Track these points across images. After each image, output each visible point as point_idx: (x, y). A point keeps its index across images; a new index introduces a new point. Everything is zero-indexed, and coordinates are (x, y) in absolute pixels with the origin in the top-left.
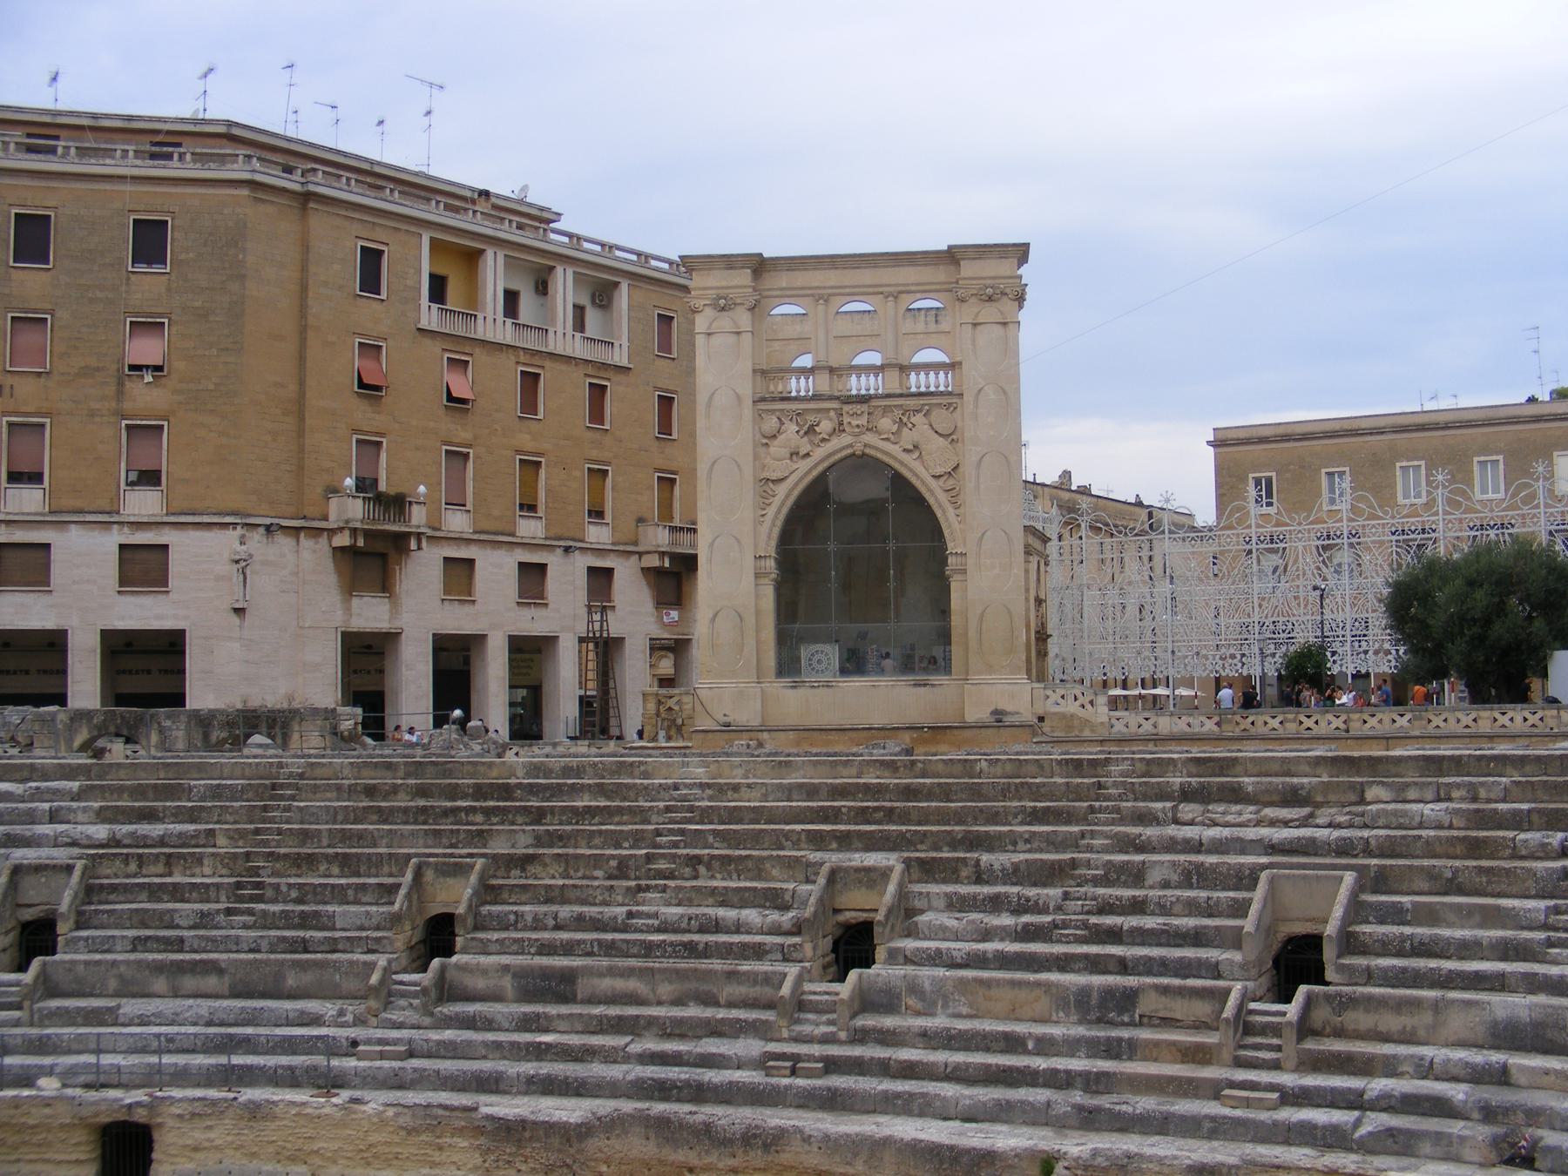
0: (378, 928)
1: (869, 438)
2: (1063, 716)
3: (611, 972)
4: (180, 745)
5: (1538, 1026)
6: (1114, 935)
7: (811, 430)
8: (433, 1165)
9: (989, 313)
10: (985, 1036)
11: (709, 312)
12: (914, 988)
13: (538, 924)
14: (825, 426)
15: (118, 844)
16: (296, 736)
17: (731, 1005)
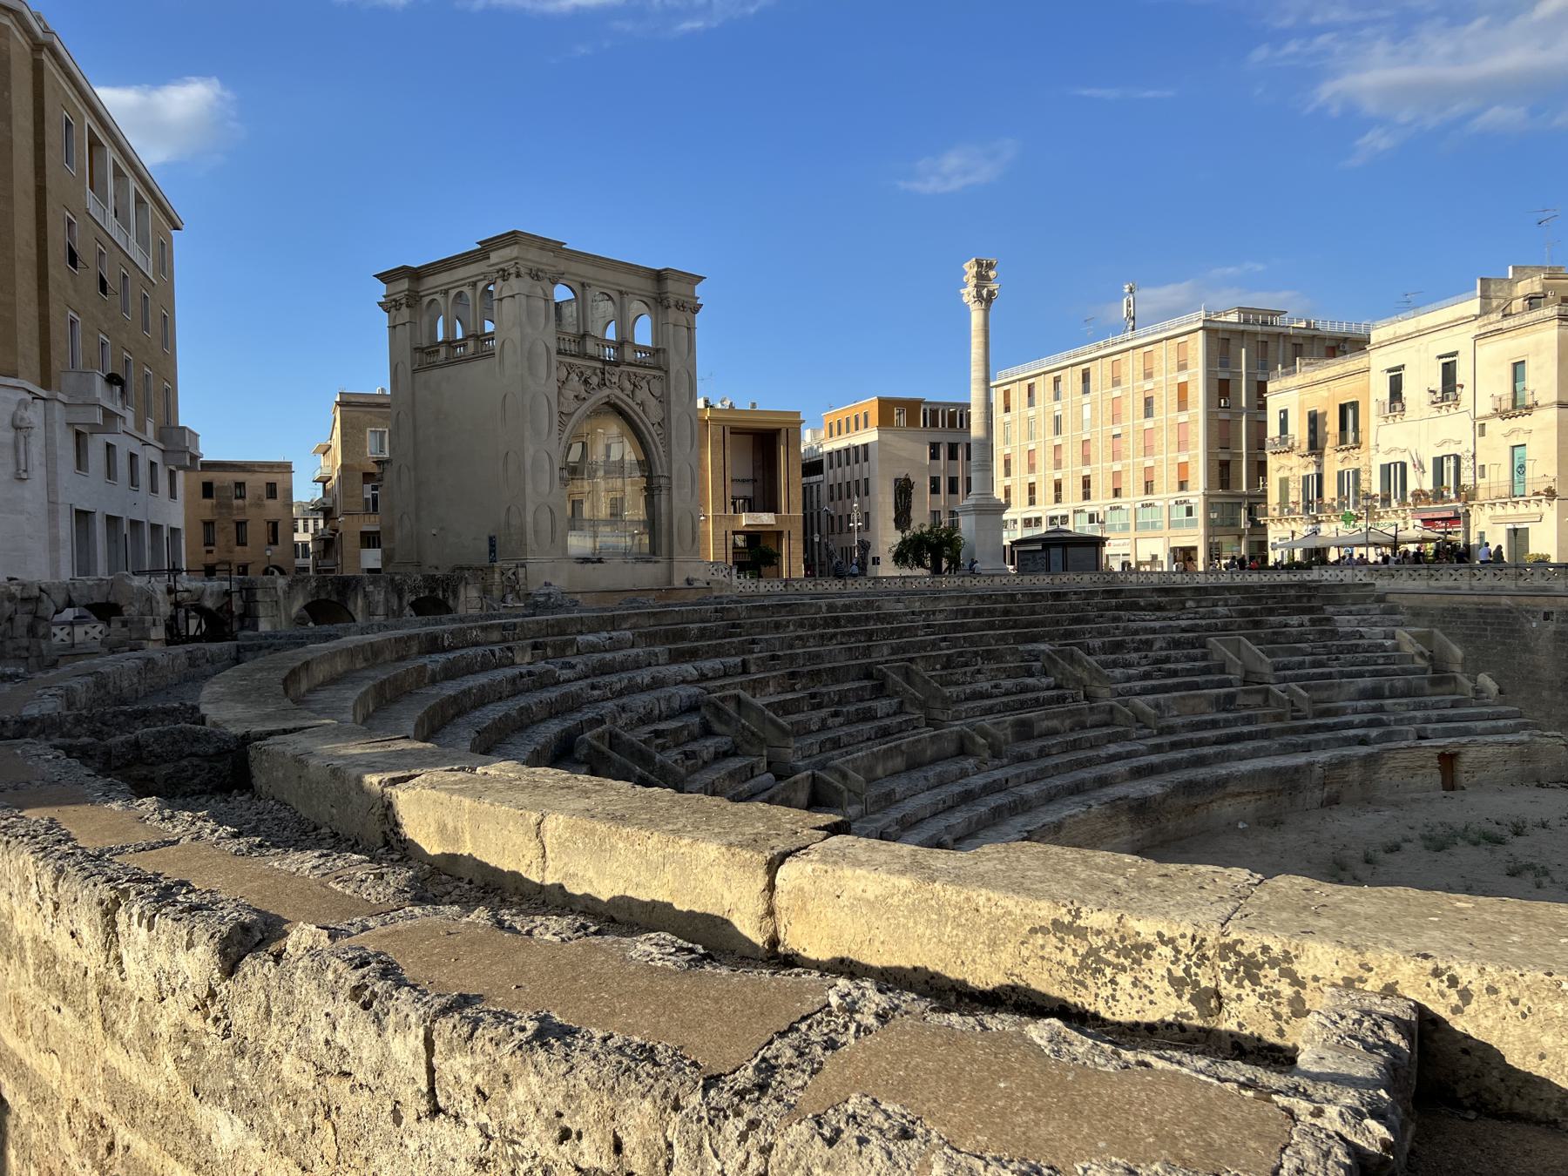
0: (895, 714)
1: (618, 392)
2: (718, 582)
3: (1048, 717)
4: (381, 610)
5: (1374, 689)
6: (1174, 673)
7: (586, 382)
8: (1116, 836)
9: (682, 317)
10: (1206, 722)
11: (528, 278)
12: (1157, 706)
13: (958, 701)
14: (595, 380)
15: (703, 677)
16: (462, 598)
17: (1092, 727)
